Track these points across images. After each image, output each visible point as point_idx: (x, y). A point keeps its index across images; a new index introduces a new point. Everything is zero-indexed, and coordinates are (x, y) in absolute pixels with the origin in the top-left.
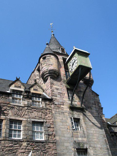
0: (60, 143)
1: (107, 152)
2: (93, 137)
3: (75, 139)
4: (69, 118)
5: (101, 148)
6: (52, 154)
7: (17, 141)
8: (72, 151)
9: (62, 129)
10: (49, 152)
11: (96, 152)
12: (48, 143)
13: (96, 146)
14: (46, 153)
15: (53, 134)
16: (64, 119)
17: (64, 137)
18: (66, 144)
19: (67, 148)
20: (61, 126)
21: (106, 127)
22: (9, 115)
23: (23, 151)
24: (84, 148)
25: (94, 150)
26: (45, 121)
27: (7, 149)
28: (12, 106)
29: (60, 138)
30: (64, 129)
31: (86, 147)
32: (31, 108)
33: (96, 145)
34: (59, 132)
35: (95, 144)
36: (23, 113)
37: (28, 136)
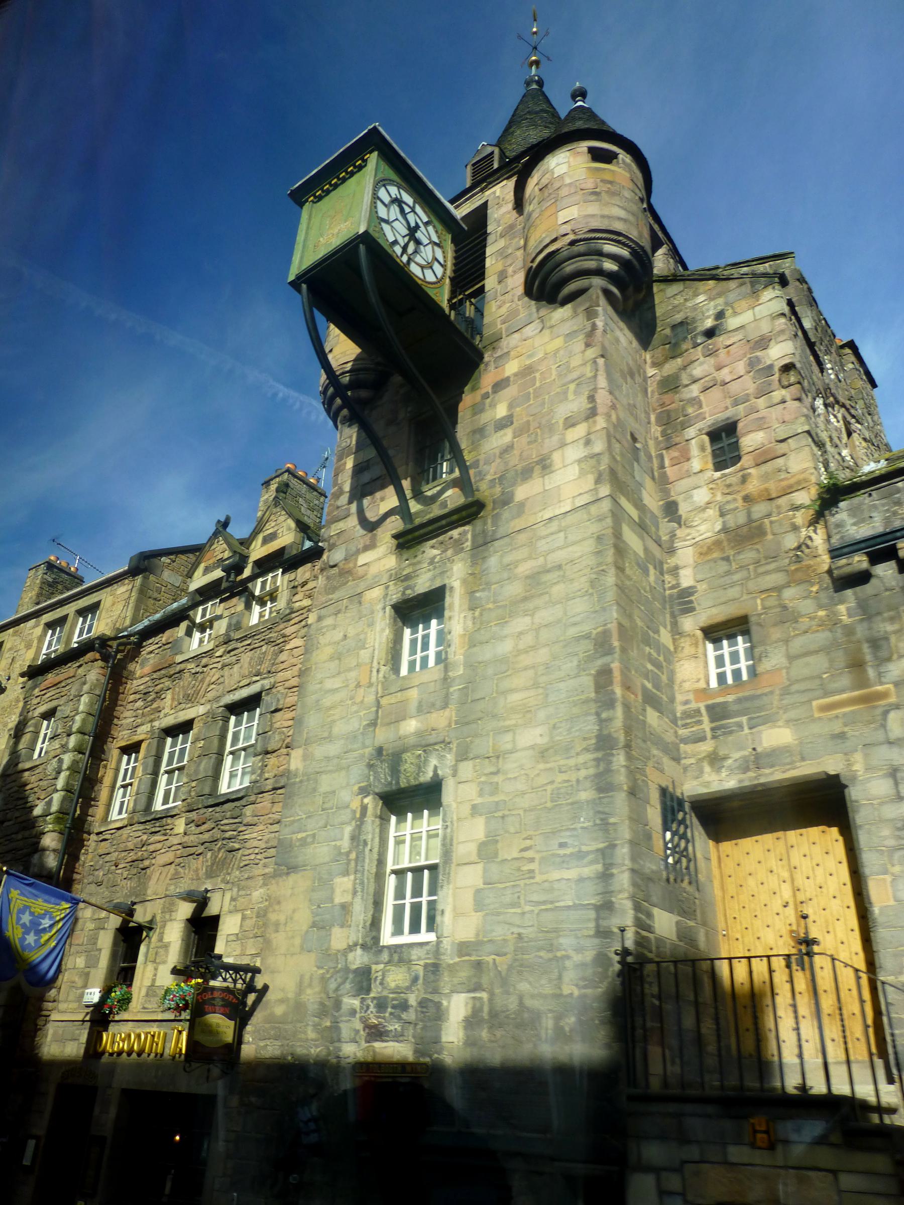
0: (301, 782)
1: (592, 771)
2: (506, 684)
3: (382, 736)
4: (381, 614)
5: (543, 753)
6: (257, 851)
7: (162, 818)
8: (345, 815)
9: (327, 701)
10: (248, 845)
11: (495, 789)
12: (253, 798)
13: (509, 746)
14: (239, 849)
15: (288, 740)
16: (351, 632)
17: (330, 738)
18: (325, 783)
19: (326, 806)
20: (329, 684)
21: (795, 528)
22: (162, 714)
23: (169, 857)
24: (422, 779)
25: (483, 779)
26: (267, 683)
27: (132, 856)
28: (178, 668)
29: (305, 757)
30: (337, 697)
31: (436, 768)
32: (237, 640)
33: (508, 737)
34: (312, 721)
35: (507, 730)
36: (208, 679)
37: (194, 784)
